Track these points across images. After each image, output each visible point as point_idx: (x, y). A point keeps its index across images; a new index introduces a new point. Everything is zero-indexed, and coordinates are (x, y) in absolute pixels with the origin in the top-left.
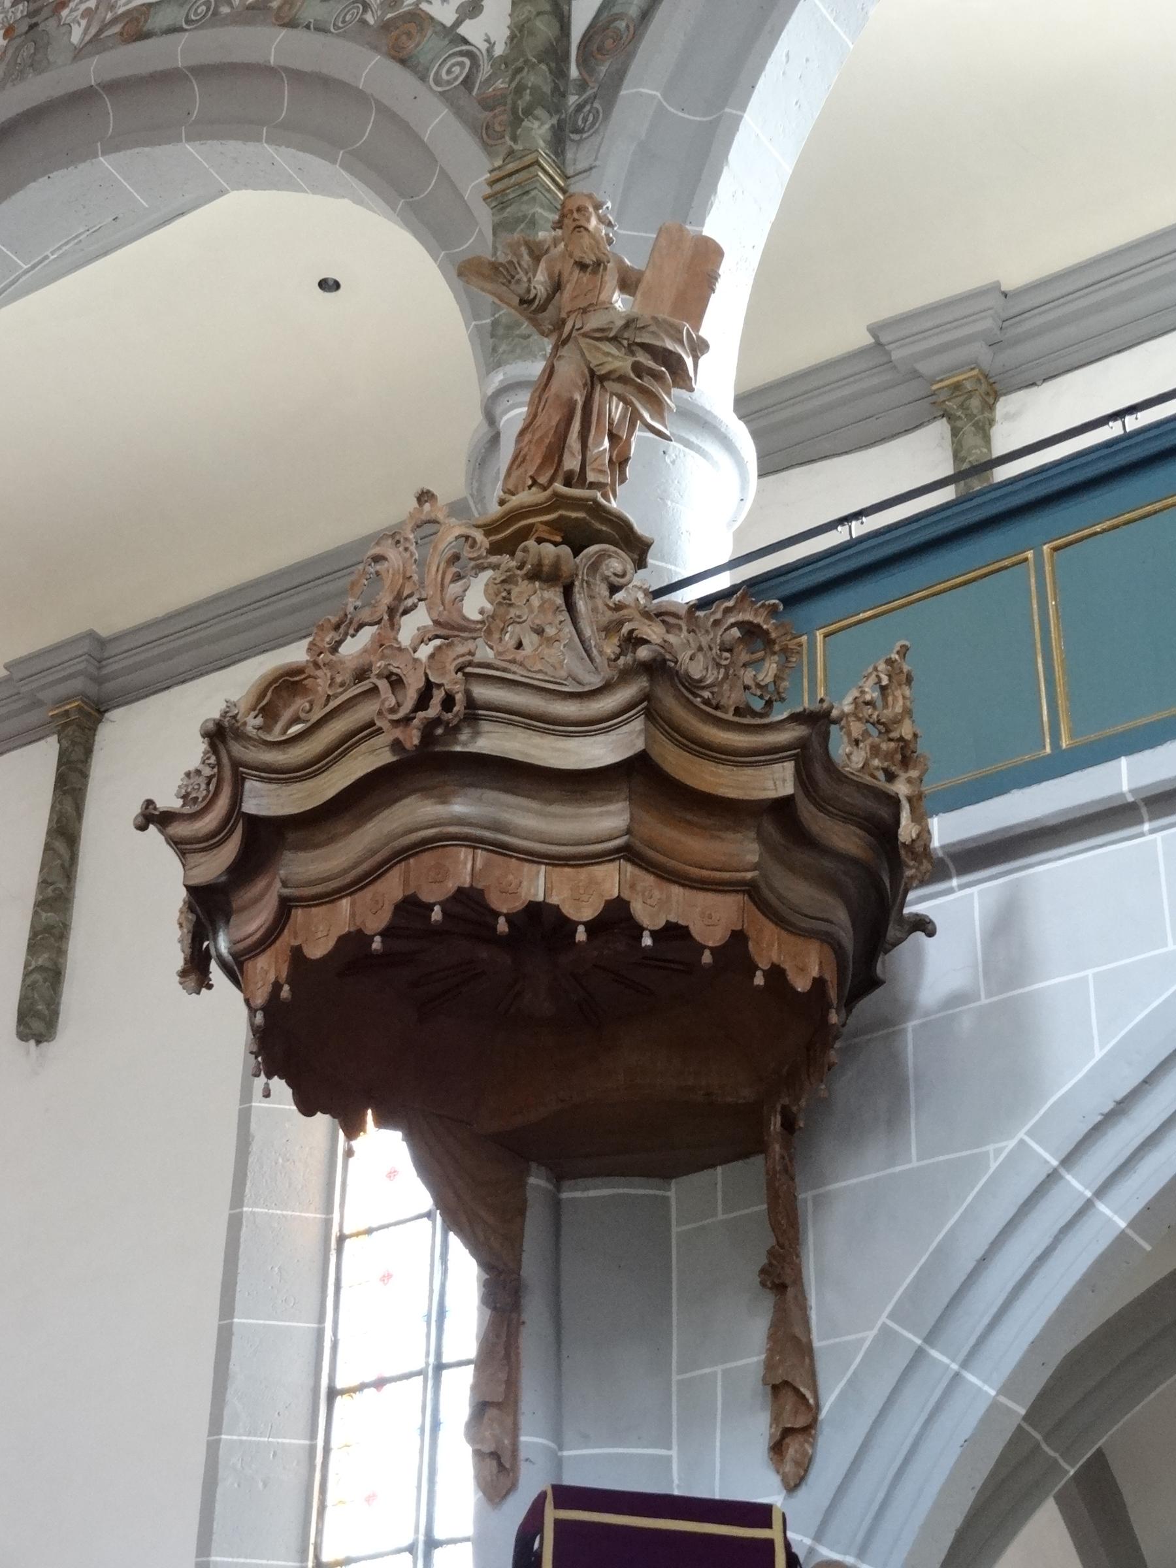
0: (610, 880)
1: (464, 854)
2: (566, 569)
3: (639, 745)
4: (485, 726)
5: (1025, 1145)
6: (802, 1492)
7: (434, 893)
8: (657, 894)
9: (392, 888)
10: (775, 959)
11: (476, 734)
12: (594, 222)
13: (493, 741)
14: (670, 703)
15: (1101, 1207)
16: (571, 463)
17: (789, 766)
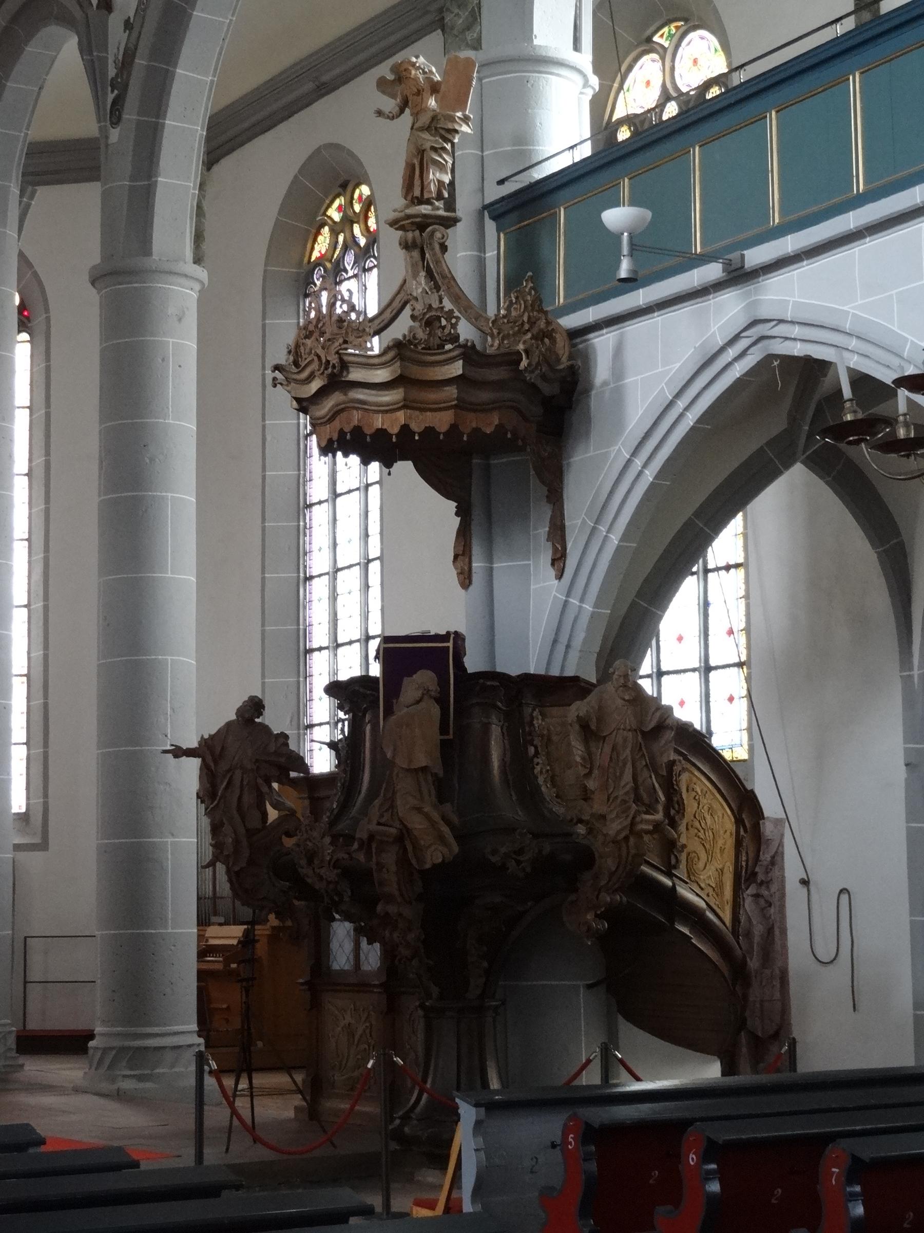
0: (401, 417)
1: (355, 412)
2: (418, 241)
3: (399, 372)
4: (351, 369)
5: (621, 450)
6: (562, 580)
7: (347, 429)
8: (421, 417)
9: (337, 424)
10: (474, 425)
11: (348, 373)
12: (413, 72)
13: (356, 375)
14: (408, 353)
15: (647, 472)
16: (417, 193)
17: (461, 362)
